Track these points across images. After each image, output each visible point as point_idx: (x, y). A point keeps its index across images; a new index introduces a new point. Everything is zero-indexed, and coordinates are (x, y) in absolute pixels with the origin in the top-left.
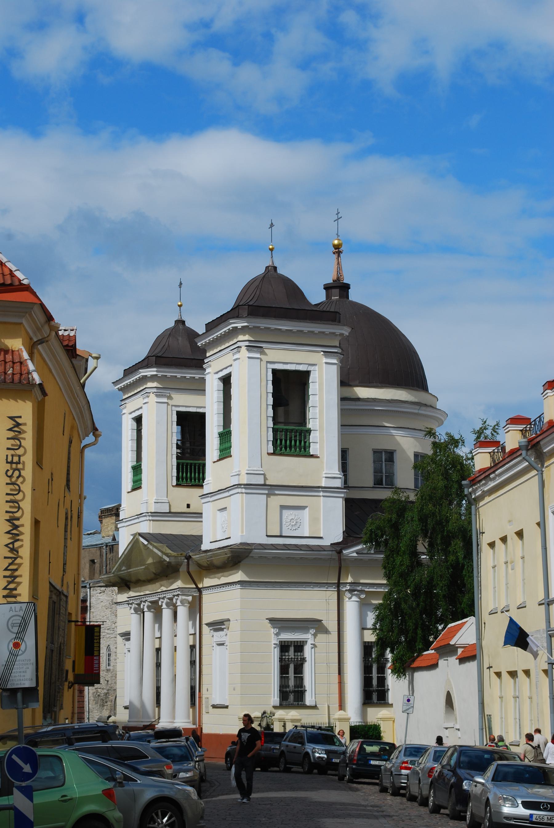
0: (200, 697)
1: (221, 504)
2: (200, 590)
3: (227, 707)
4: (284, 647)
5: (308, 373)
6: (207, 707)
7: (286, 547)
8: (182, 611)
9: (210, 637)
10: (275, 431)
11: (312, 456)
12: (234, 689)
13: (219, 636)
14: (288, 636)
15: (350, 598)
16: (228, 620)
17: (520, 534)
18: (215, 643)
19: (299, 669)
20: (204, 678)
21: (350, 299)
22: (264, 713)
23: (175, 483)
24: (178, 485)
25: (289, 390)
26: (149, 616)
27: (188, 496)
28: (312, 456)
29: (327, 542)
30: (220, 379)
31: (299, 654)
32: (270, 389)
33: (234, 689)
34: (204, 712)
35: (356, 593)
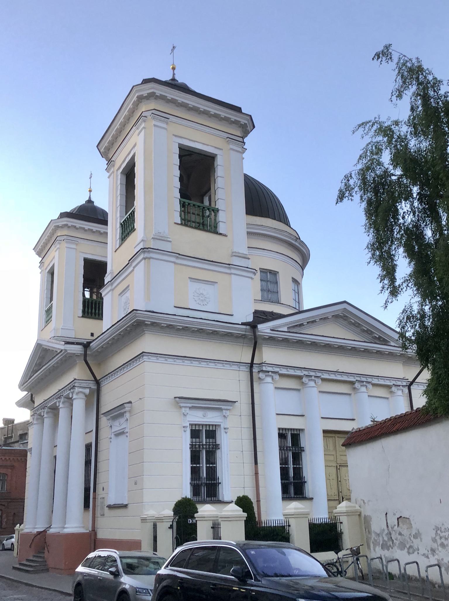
0: (94, 498)
2: (98, 383)
3: (125, 506)
6: (102, 508)
8: (79, 405)
11: (221, 234)
12: (136, 484)
14: (200, 418)
16: (130, 402)
18: (113, 434)
20: (99, 465)
23: (81, 315)
24: (82, 317)
26: (47, 422)
28: (221, 234)
31: (211, 440)
33: (136, 484)
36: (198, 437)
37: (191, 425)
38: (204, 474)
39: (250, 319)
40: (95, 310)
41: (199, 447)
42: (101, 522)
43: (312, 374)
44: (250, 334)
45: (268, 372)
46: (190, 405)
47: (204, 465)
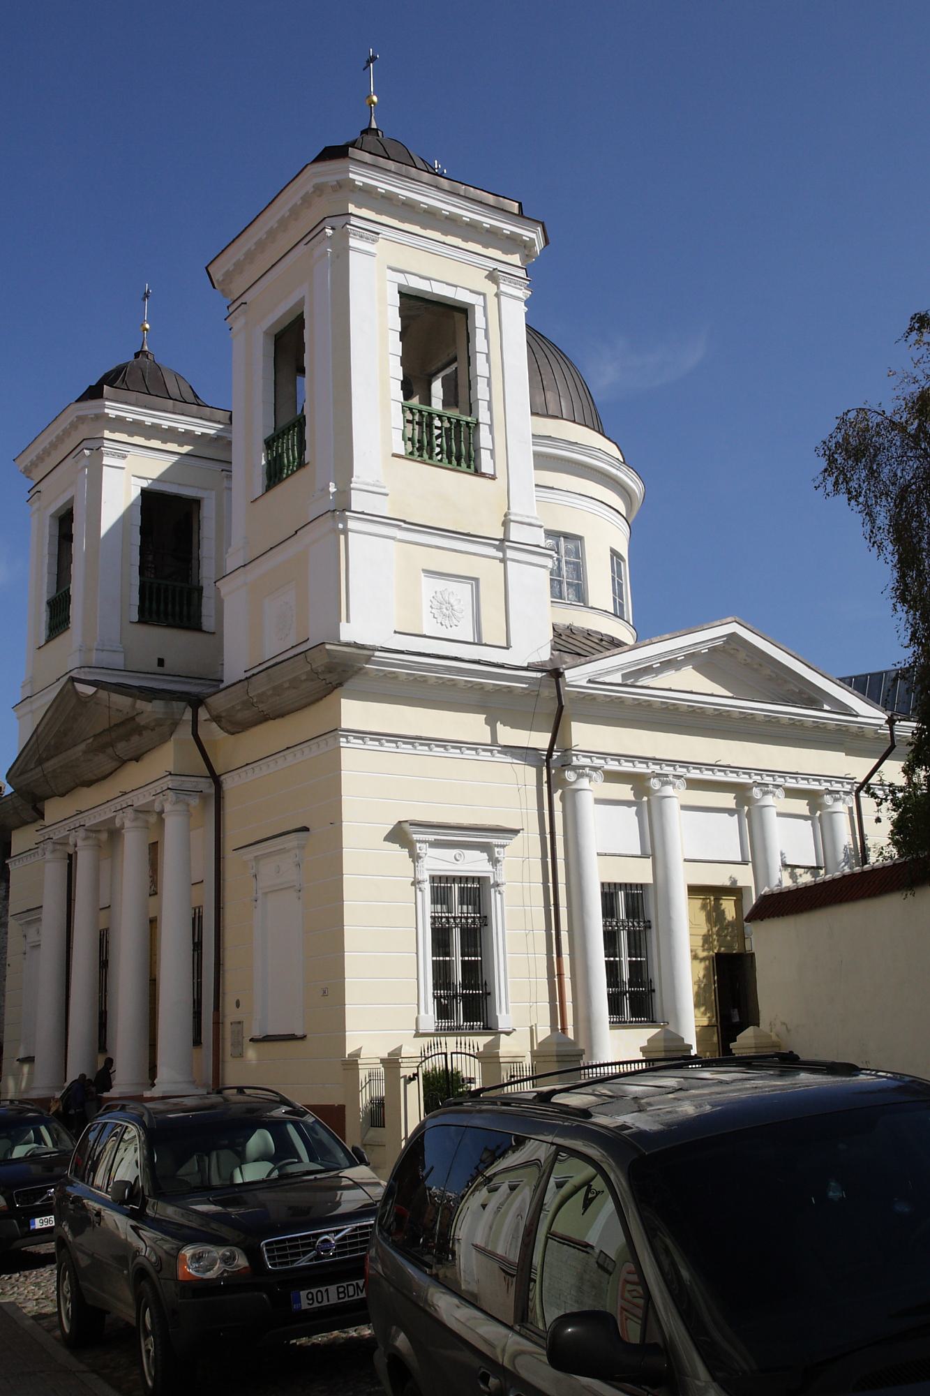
0: (217, 1023)
4: (441, 888)
6: (238, 1044)
11: (483, 475)
23: (136, 618)
24: (140, 622)
34: (228, 1058)
37: (433, 879)
40: (166, 605)
41: (448, 922)
43: (667, 770)
44: (548, 692)
45: (583, 767)
46: (432, 838)
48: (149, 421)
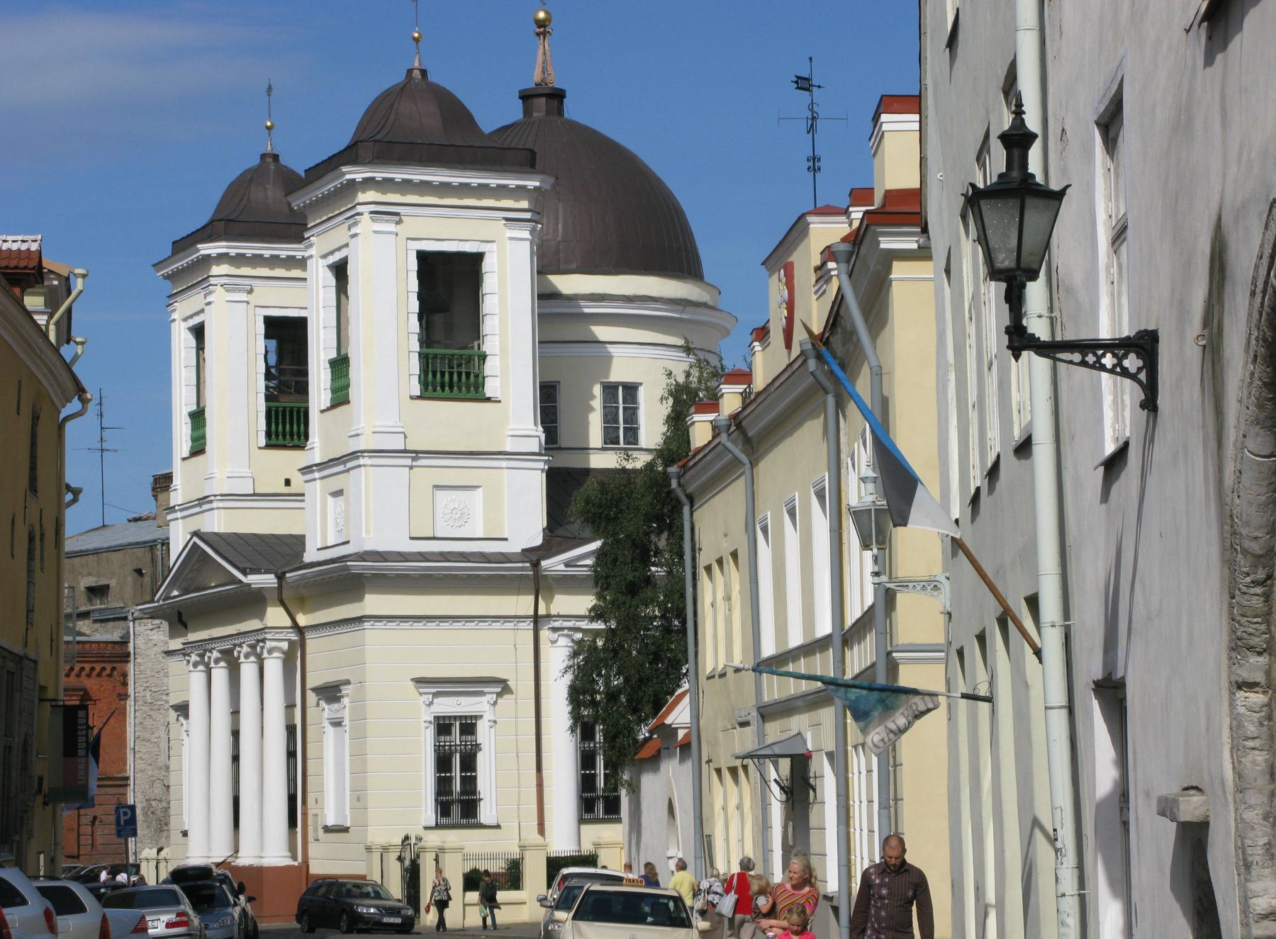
1: (335, 483)
4: (443, 726)
5: (479, 257)
6: (316, 830)
7: (444, 556)
8: (274, 667)
9: (321, 713)
10: (424, 358)
11: (489, 400)
13: (328, 710)
15: (553, 642)
17: (734, 555)
19: (469, 763)
21: (566, 115)
22: (407, 838)
23: (263, 442)
24: (268, 446)
25: (448, 287)
27: (288, 461)
28: (489, 400)
29: (514, 547)
30: (330, 267)
32: (414, 284)
34: (310, 838)
35: (566, 632)
36: (449, 733)
38: (457, 786)
39: (538, 541)
42: (313, 849)
46: (435, 690)
47: (457, 773)
48: (267, 253)
